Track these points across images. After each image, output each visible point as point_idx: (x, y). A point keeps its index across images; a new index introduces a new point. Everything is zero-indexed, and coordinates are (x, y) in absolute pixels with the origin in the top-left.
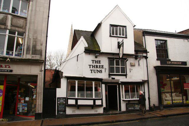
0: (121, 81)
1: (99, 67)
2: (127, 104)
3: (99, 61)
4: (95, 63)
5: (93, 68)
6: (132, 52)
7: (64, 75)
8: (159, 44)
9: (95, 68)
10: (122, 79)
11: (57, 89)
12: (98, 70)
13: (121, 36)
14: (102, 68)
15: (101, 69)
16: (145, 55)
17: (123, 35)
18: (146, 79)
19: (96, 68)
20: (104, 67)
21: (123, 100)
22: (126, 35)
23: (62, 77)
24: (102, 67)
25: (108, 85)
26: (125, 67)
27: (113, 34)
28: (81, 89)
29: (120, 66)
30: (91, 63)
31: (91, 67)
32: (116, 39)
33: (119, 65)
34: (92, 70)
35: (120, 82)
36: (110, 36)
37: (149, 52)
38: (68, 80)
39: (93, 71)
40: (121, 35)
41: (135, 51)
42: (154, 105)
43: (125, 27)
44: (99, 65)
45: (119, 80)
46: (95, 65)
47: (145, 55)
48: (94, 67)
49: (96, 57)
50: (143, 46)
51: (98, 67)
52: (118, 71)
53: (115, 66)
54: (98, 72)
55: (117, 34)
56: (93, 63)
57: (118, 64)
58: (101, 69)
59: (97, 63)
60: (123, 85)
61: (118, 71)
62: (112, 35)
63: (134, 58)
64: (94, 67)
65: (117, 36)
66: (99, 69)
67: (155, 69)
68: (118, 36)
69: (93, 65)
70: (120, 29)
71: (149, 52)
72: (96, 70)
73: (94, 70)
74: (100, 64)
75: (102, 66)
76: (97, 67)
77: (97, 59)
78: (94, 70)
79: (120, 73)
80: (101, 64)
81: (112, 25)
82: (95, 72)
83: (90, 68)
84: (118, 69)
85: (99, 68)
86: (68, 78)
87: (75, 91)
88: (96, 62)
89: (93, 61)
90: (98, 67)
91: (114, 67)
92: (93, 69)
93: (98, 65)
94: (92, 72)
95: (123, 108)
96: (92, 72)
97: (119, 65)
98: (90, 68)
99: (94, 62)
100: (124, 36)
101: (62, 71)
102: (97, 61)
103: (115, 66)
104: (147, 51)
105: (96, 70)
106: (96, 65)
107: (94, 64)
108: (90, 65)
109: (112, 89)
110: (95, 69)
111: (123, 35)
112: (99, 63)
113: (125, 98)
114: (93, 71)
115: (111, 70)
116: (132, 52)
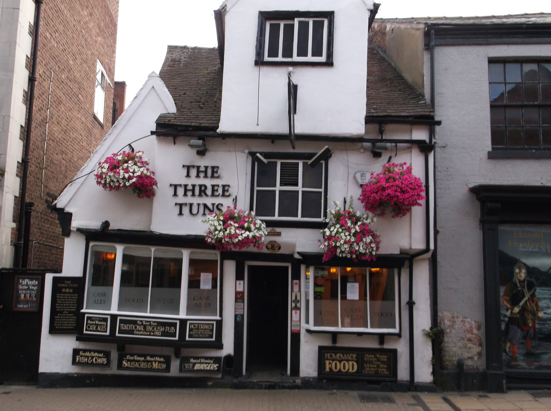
0: (299, 249)
1: (213, 191)
2: (321, 349)
3: (213, 168)
4: (198, 176)
5: (185, 195)
6: (354, 124)
7: (75, 224)
8: (514, 75)
9: (193, 195)
10: (301, 241)
11: (202, 274)
12: (205, 206)
13: (310, 58)
14: (223, 195)
15: (217, 201)
16: (420, 135)
17: (317, 52)
18: (418, 245)
19: (200, 195)
20: (233, 191)
21: (308, 331)
22: (330, 55)
23: (67, 232)
24: (224, 191)
25: (250, 267)
26: (322, 190)
27: (273, 52)
28: (134, 277)
29: (300, 188)
30: (180, 178)
31: (180, 191)
32: (282, 72)
33: (297, 185)
34: (181, 205)
35: (297, 256)
36: (259, 62)
37: (439, 123)
38: (91, 244)
39: (186, 210)
40: (306, 55)
41: (369, 120)
42: (460, 364)
43: (330, 15)
44: (213, 186)
45: (294, 246)
46: (194, 186)
47: (420, 135)
48: (193, 191)
49: (201, 153)
50: (423, 96)
51: (209, 192)
52: (288, 206)
53: (278, 188)
54: (207, 212)
55: (288, 52)
56: (188, 176)
57: (290, 178)
58: (217, 201)
59: (206, 176)
60: (312, 265)
61: (288, 206)
62: (267, 59)
63: (365, 149)
64: (190, 193)
65: (289, 60)
66: (209, 201)
67: (479, 199)
68: (296, 58)
69: (186, 186)
70: (304, 27)
71: (439, 123)
72: (199, 205)
73: (191, 205)
74: (215, 182)
75: (224, 186)
76: (203, 190)
77: (203, 162)
78: (191, 205)
79: (299, 218)
80: (219, 182)
81: (265, 16)
82: (195, 211)
83: (175, 194)
84: (289, 203)
85: (213, 195)
86: (89, 235)
87: (112, 285)
88: (198, 172)
89: (188, 168)
90: (209, 192)
91: (275, 191)
92: (189, 199)
93: (208, 183)
94: (181, 214)
95: (308, 366)
96: (181, 214)
97: (297, 185)
98: (175, 194)
99: (193, 172)
100: (323, 59)
101: (67, 210)
102: (206, 167)
103: (278, 188)
104: (432, 118)
105: (199, 205)
106: (200, 186)
107: (190, 182)
108: (176, 186)
109: (269, 282)
110: (195, 201)
111: (317, 52)
112: (213, 177)
113: (316, 324)
114: (186, 210)
115: (262, 203)
116: (354, 124)
